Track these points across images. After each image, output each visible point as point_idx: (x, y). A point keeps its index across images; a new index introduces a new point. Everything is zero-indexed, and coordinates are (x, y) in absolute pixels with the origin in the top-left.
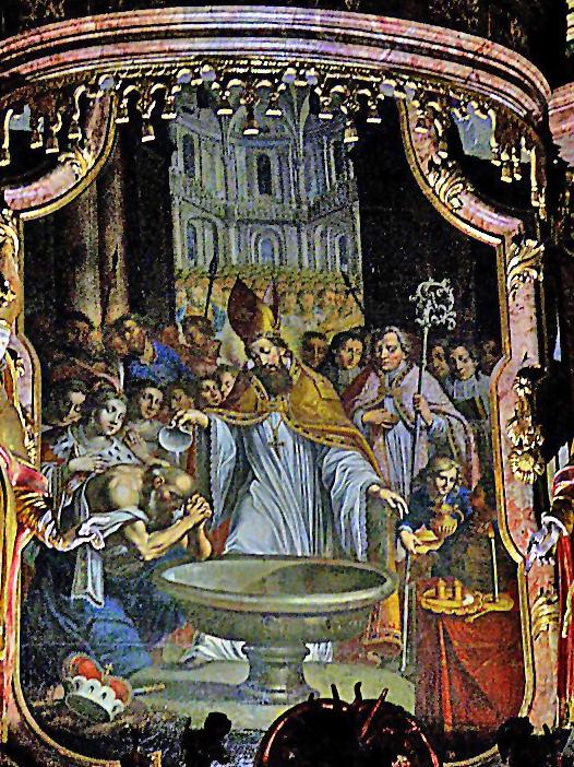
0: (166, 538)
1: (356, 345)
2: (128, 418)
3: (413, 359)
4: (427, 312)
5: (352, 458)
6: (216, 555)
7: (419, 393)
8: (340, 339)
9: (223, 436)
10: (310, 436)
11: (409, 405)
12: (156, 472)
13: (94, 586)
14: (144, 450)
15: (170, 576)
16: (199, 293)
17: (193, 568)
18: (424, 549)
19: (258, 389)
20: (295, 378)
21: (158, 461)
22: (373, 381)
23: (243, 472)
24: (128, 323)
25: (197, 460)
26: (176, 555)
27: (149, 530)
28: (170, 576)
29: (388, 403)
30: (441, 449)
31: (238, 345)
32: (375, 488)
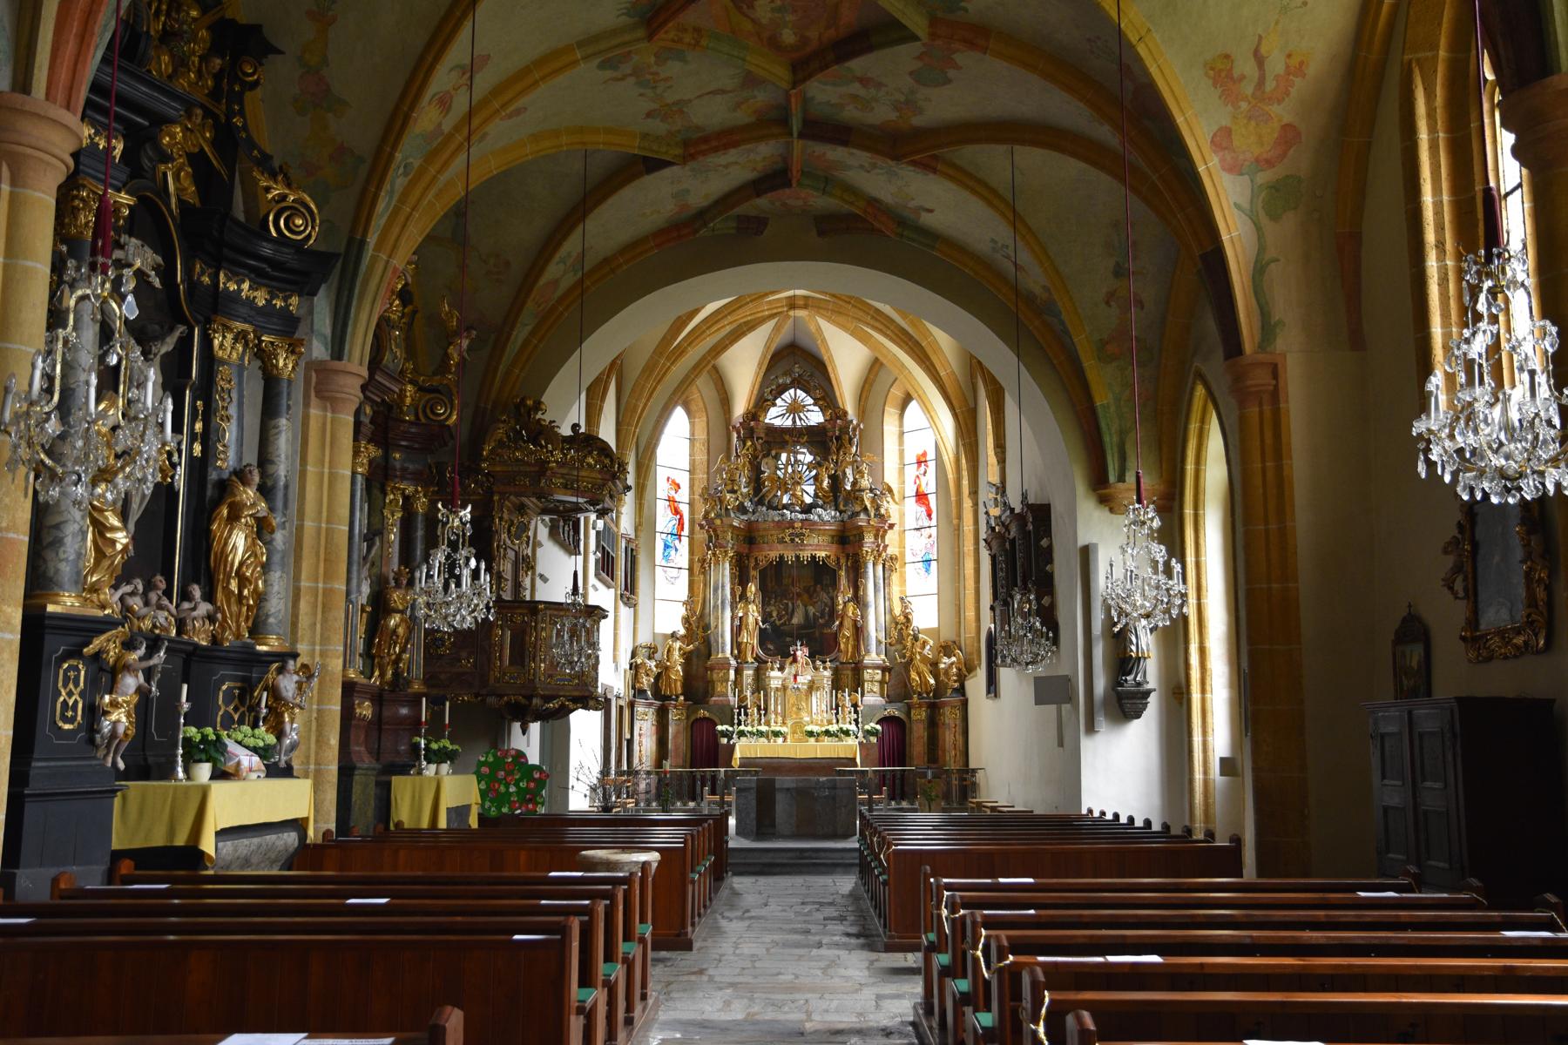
9: (790, 605)
23: (793, 611)
25: (786, 609)
26: (782, 624)
30: (826, 605)
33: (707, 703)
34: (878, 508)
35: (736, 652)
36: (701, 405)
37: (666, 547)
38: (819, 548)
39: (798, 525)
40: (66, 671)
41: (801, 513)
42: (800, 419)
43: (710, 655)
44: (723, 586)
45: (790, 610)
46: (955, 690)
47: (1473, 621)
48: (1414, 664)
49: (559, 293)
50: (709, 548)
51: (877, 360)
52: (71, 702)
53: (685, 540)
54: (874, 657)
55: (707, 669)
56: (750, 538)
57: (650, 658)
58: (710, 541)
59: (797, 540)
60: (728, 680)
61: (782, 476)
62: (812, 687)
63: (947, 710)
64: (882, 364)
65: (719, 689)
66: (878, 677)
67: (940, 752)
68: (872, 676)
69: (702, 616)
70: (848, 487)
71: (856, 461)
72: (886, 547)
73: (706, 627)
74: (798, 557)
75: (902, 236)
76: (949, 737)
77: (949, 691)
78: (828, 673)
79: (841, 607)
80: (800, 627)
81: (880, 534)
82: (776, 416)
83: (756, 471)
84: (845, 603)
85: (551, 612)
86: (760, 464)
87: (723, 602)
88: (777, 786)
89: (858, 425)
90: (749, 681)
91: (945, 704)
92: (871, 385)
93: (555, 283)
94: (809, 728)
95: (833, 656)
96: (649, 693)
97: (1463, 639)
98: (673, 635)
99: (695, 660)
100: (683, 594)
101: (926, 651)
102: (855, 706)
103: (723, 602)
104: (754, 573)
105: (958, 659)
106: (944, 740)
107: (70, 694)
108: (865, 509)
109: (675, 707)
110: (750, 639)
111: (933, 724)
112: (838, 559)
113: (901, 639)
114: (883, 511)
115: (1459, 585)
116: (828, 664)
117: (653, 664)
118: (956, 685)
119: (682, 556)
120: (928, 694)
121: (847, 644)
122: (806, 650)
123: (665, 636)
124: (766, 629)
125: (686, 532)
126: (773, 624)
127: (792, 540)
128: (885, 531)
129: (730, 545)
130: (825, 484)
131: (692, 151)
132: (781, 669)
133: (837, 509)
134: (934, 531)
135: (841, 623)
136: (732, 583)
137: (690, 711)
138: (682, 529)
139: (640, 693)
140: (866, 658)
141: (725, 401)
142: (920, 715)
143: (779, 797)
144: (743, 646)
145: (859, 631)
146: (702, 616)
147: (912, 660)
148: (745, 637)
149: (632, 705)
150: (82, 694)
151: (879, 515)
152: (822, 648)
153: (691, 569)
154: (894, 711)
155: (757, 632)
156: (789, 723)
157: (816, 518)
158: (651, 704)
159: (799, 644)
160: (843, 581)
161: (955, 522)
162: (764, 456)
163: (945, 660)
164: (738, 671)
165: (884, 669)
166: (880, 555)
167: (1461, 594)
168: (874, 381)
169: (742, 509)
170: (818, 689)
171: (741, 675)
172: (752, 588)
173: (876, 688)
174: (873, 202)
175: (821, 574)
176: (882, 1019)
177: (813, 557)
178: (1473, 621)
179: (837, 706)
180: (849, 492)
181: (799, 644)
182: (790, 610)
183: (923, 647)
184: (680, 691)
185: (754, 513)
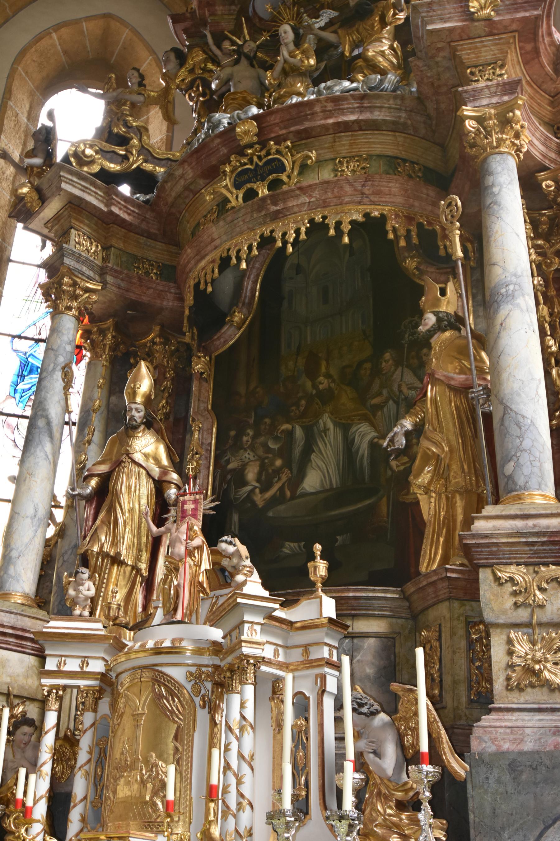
0: (269, 494)
1: (368, 365)
2: (254, 437)
3: (398, 363)
4: (407, 336)
5: (364, 428)
6: (293, 497)
7: (401, 381)
8: (360, 364)
9: (299, 432)
10: (343, 421)
11: (395, 388)
12: (266, 461)
13: (235, 528)
14: (260, 452)
15: (270, 514)
16: (291, 364)
17: (282, 507)
18: (402, 468)
19: (317, 404)
20: (336, 392)
21: (267, 455)
22: (377, 382)
23: (308, 450)
24: (258, 390)
27: (262, 491)
28: (270, 514)
29: (385, 392)
31: (309, 384)
32: (376, 440)
45: (297, 451)
127: (250, 195)
182: (297, 451)
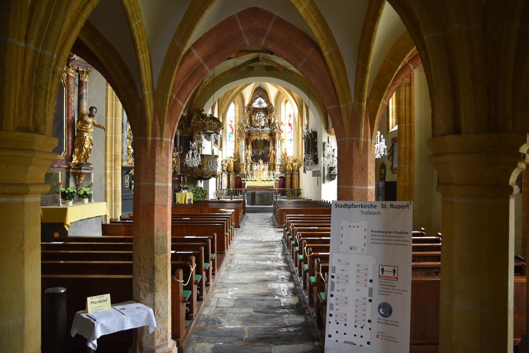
23: (259, 151)
26: (257, 155)
33: (239, 173)
34: (279, 128)
35: (246, 161)
36: (237, 101)
37: (229, 136)
38: (265, 137)
39: (260, 131)
40: (126, 177)
41: (261, 128)
42: (261, 106)
43: (240, 162)
44: (243, 146)
46: (297, 171)
47: (392, 166)
48: (383, 173)
49: (207, 84)
50: (239, 137)
51: (279, 92)
52: (127, 182)
53: (234, 135)
54: (278, 162)
55: (239, 165)
56: (249, 134)
57: (226, 163)
58: (240, 135)
59: (260, 135)
60: (244, 168)
61: (257, 119)
62: (264, 170)
63: (295, 175)
64: (281, 93)
65: (242, 170)
66: (279, 167)
67: (293, 185)
68: (277, 167)
69: (238, 153)
70: (272, 122)
71: (274, 116)
72: (281, 136)
73: (239, 155)
74: (260, 139)
75: (285, 72)
76: (295, 182)
77: (295, 171)
78: (267, 166)
79: (270, 151)
80: (261, 155)
81: (280, 133)
82: (255, 105)
83: (251, 118)
84: (271, 150)
85: (207, 157)
86: (251, 116)
87: (243, 150)
88: (256, 193)
89: (275, 107)
90: (249, 168)
91: (294, 174)
92: (278, 97)
93: (206, 82)
94: (263, 179)
95: (268, 162)
96: (226, 171)
97: (390, 169)
98: (231, 157)
99: (236, 163)
100: (234, 148)
101: (290, 161)
102: (274, 174)
103: (243, 150)
104: (250, 143)
105: (298, 163)
106: (294, 182)
107: (127, 181)
108: (276, 128)
109: (232, 174)
110: (249, 158)
111: (292, 178)
112: (270, 139)
113: (284, 158)
114: (280, 128)
115: (390, 159)
116: (267, 164)
117: (226, 164)
118: (297, 169)
119: (233, 138)
120: (290, 171)
121: (272, 159)
122: (262, 161)
123: (229, 157)
124: (253, 156)
125: (234, 132)
126: (254, 155)
127: (259, 135)
128: (281, 133)
129: (244, 136)
130: (267, 122)
131: (238, 55)
132: (256, 165)
133: (270, 128)
134: (293, 133)
135: (271, 155)
136: (245, 145)
137: (235, 175)
138: (233, 132)
139: (224, 171)
140: (276, 163)
141: (243, 101)
142: (289, 176)
143: (257, 196)
144: (247, 160)
145: (275, 156)
146: (238, 153)
147: (287, 163)
148: (248, 158)
149: (222, 174)
150: (129, 181)
151: (280, 129)
152: (266, 160)
153: (235, 142)
154: (283, 175)
155: (251, 156)
156: (258, 178)
157: (265, 130)
158: (226, 173)
159: (261, 159)
160: (271, 145)
161: (298, 131)
162: (252, 115)
163: (295, 163)
164: (246, 166)
165: (280, 166)
166: (280, 139)
167: (391, 160)
168: (279, 96)
169: (247, 127)
170: (265, 170)
171: (247, 167)
172: (250, 146)
173: (279, 170)
174: (278, 64)
175: (266, 143)
176: (276, 239)
177: (264, 139)
178: (392, 166)
179: (269, 174)
180: (273, 124)
181: (261, 159)
183: (290, 160)
184: (233, 170)
185: (250, 128)
